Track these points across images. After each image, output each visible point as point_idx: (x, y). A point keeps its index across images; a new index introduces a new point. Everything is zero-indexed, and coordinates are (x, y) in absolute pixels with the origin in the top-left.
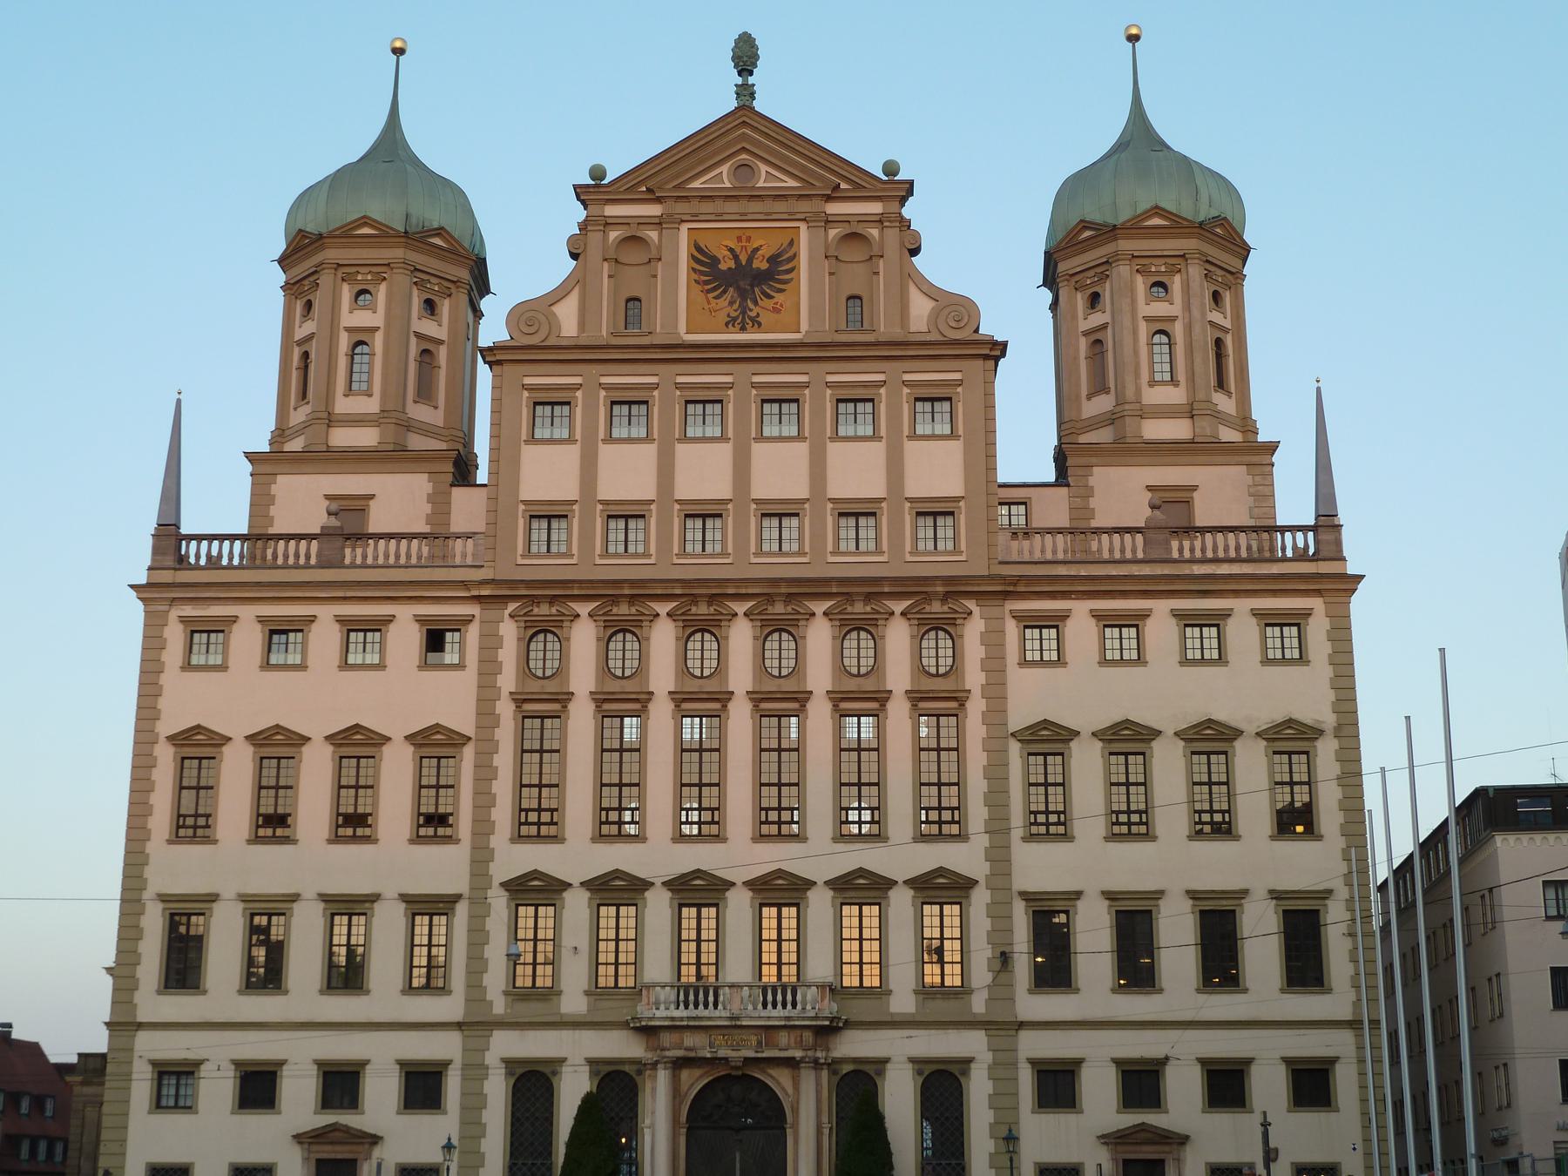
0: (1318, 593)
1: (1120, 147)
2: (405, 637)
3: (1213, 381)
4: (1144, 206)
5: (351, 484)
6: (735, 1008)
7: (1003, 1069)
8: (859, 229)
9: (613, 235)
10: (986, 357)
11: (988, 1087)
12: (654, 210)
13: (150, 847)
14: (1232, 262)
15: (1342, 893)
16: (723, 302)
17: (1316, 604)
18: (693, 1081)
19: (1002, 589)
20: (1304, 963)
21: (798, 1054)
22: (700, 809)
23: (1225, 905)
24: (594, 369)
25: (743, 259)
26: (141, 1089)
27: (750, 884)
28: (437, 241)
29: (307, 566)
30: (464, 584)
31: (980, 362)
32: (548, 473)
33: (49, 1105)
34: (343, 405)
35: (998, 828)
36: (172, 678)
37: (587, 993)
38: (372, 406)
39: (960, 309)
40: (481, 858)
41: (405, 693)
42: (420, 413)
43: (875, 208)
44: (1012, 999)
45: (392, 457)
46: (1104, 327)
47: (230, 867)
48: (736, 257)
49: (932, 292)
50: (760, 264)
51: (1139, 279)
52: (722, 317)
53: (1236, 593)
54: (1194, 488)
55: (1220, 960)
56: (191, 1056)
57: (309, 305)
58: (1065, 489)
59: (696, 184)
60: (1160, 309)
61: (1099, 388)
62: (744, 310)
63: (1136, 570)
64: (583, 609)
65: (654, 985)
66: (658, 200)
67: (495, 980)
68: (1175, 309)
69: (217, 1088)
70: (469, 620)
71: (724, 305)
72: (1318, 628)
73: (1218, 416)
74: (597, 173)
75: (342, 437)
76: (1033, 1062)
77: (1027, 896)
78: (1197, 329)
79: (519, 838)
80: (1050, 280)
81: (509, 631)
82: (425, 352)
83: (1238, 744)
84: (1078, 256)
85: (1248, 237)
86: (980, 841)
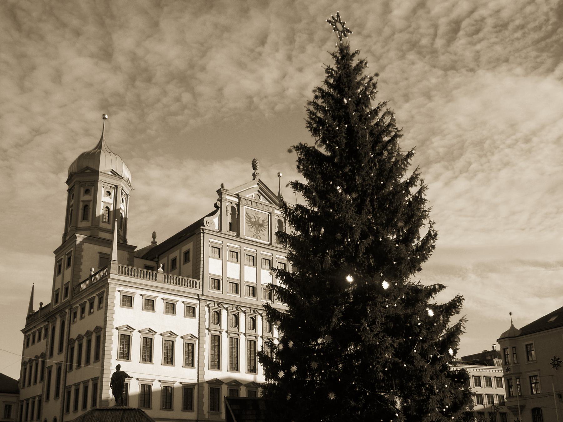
16: (253, 230)
25: (257, 219)
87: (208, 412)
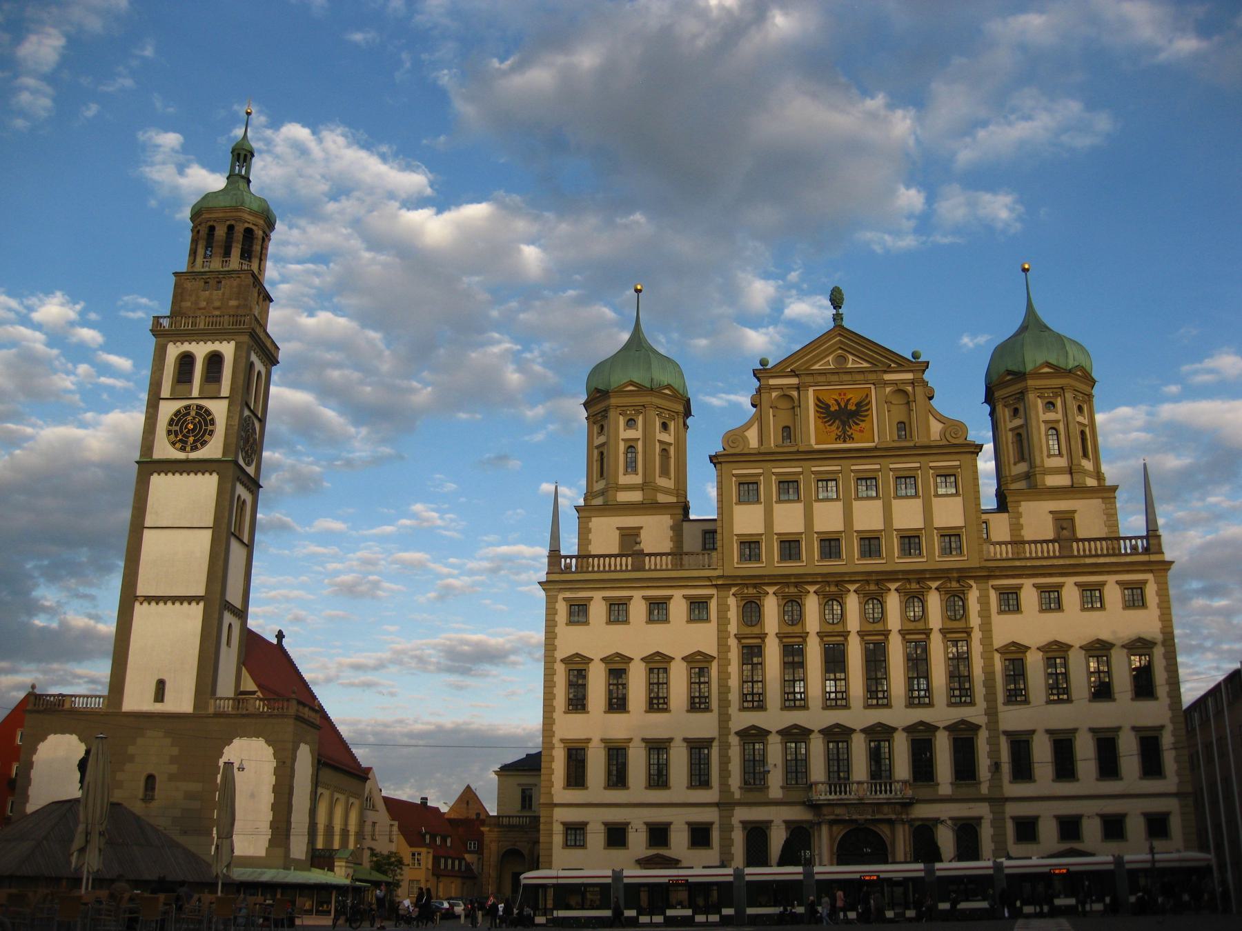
0: (1151, 571)
1: (1023, 329)
2: (678, 607)
3: (1081, 453)
4: (1040, 361)
5: (630, 521)
6: (861, 793)
7: (998, 823)
8: (902, 387)
9: (774, 394)
10: (973, 453)
11: (991, 831)
12: (794, 381)
13: (555, 715)
14: (1086, 388)
15: (1170, 727)
16: (834, 428)
17: (1149, 576)
18: (840, 832)
19: (986, 574)
20: (1151, 764)
21: (894, 817)
22: (836, 692)
23: (1110, 735)
24: (769, 465)
25: (843, 405)
26: (558, 839)
27: (863, 731)
28: (667, 391)
29: (627, 571)
30: (709, 578)
31: (969, 456)
32: (747, 520)
33: (449, 841)
34: (623, 480)
35: (990, 696)
36: (562, 629)
37: (782, 787)
38: (637, 479)
39: (955, 427)
40: (724, 719)
41: (682, 636)
42: (662, 482)
43: (910, 376)
44: (1001, 787)
45: (649, 507)
46: (1021, 426)
47: (595, 726)
48: (839, 404)
49: (941, 419)
50: (852, 407)
51: (1039, 400)
52: (833, 436)
53: (1109, 573)
54: (1074, 512)
55: (1108, 765)
56: (585, 820)
57: (602, 427)
58: (1006, 515)
59: (816, 367)
60: (1051, 416)
61: (1021, 458)
62: (844, 432)
63: (1056, 562)
64: (771, 590)
65: (816, 784)
66: (797, 376)
67: (735, 781)
68: (1059, 416)
69: (596, 837)
70: (711, 597)
71: (834, 429)
72: (1151, 591)
73: (1085, 472)
74: (763, 362)
75: (623, 497)
76: (1013, 818)
77: (1006, 733)
78: (1071, 426)
79: (743, 709)
80: (989, 398)
81: (732, 602)
82: (664, 450)
83: (1113, 652)
84: (1006, 387)
85: (1093, 375)
86: (981, 704)
87: (740, 788)
